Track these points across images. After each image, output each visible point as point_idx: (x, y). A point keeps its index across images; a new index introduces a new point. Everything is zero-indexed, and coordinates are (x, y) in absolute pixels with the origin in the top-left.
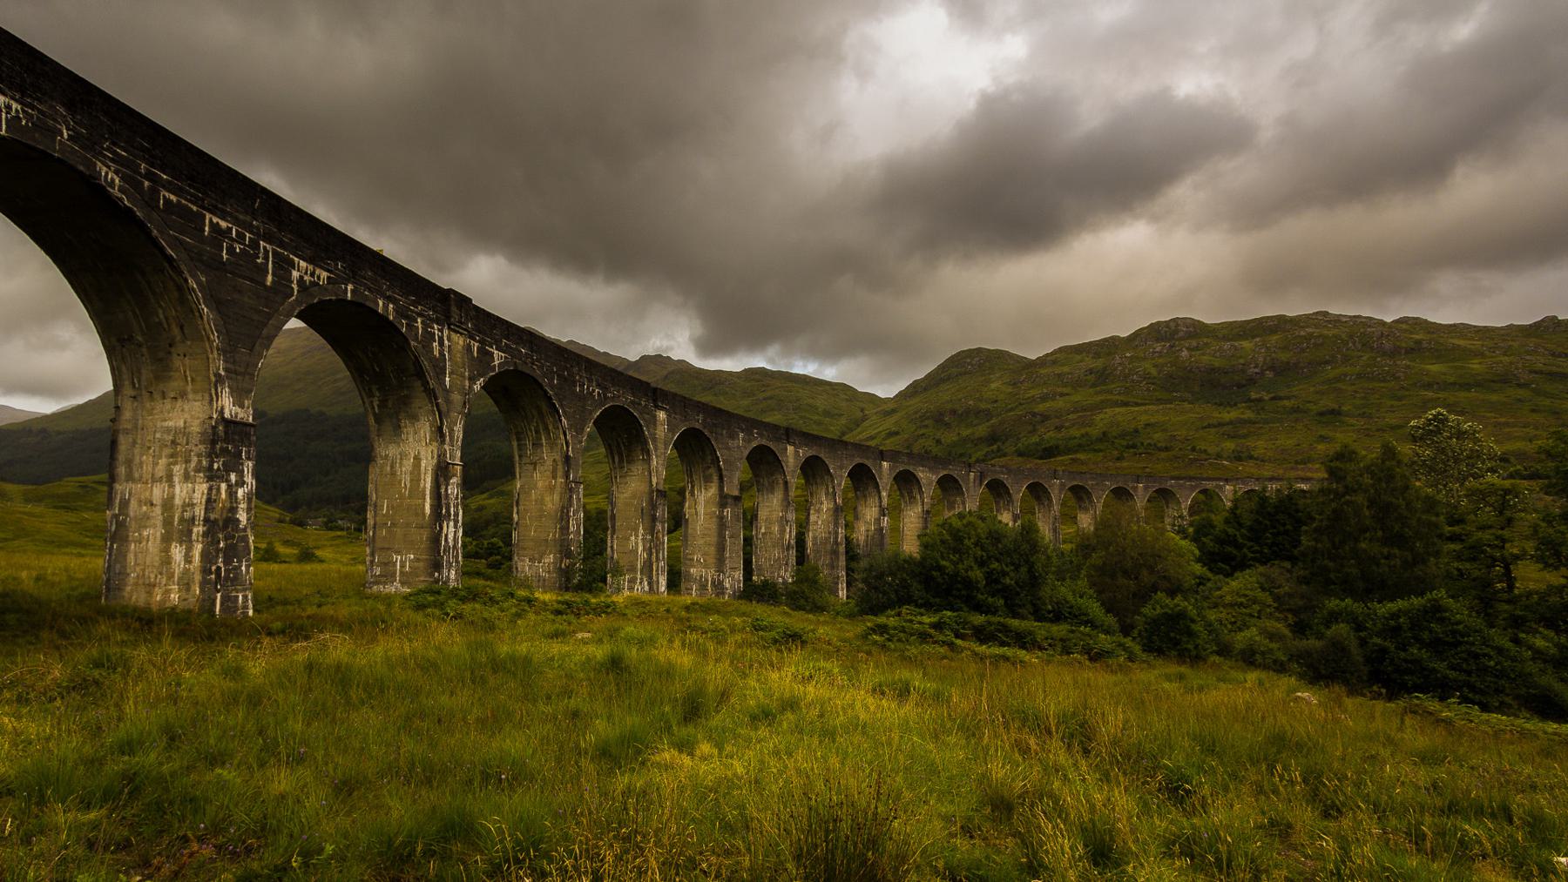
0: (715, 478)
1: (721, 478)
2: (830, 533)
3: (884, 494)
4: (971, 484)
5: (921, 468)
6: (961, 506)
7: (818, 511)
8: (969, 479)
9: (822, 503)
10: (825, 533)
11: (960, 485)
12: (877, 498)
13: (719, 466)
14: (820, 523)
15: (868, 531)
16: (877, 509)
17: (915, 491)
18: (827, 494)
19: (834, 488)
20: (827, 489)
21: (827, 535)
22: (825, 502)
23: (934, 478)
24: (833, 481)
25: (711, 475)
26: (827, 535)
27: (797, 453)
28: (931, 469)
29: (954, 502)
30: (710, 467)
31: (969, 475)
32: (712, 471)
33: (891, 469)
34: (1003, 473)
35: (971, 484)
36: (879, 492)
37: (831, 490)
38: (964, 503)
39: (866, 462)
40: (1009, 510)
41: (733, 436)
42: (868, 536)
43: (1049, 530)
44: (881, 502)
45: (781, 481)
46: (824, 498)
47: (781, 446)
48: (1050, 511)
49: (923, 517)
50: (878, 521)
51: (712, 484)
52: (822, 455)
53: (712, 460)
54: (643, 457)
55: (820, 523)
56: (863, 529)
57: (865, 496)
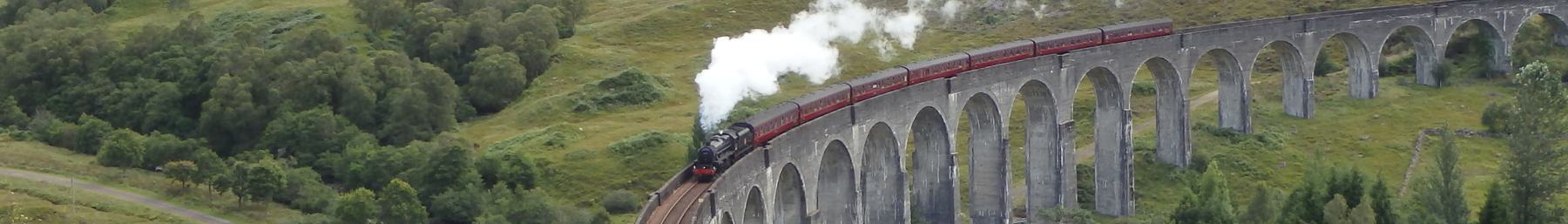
0: (797, 200)
1: (803, 199)
2: (892, 206)
3: (952, 136)
4: (1063, 85)
5: (996, 85)
6: (1049, 117)
7: (877, 179)
8: (1059, 80)
9: (881, 169)
10: (886, 205)
11: (1048, 91)
12: (943, 142)
13: (802, 189)
14: (879, 193)
15: (932, 184)
16: (944, 155)
17: (989, 113)
18: (888, 158)
19: (897, 152)
20: (888, 150)
21: (889, 209)
22: (885, 168)
23: (1014, 92)
24: (895, 143)
25: (792, 196)
26: (889, 209)
27: (861, 129)
28: (1009, 82)
29: (1040, 110)
30: (790, 189)
31: (1059, 73)
32: (794, 193)
33: (959, 99)
34: (1107, 57)
35: (1063, 85)
36: (946, 135)
37: (892, 154)
38: (1053, 113)
39: (930, 103)
41: (810, 153)
42: (931, 191)
43: (1174, 121)
44: (948, 147)
45: (845, 169)
46: (883, 163)
47: (847, 132)
48: (1175, 94)
49: (1000, 149)
50: (946, 172)
51: (793, 206)
52: (884, 120)
53: (794, 183)
54: (756, 215)
55: (879, 193)
56: (925, 181)
57: (927, 139)
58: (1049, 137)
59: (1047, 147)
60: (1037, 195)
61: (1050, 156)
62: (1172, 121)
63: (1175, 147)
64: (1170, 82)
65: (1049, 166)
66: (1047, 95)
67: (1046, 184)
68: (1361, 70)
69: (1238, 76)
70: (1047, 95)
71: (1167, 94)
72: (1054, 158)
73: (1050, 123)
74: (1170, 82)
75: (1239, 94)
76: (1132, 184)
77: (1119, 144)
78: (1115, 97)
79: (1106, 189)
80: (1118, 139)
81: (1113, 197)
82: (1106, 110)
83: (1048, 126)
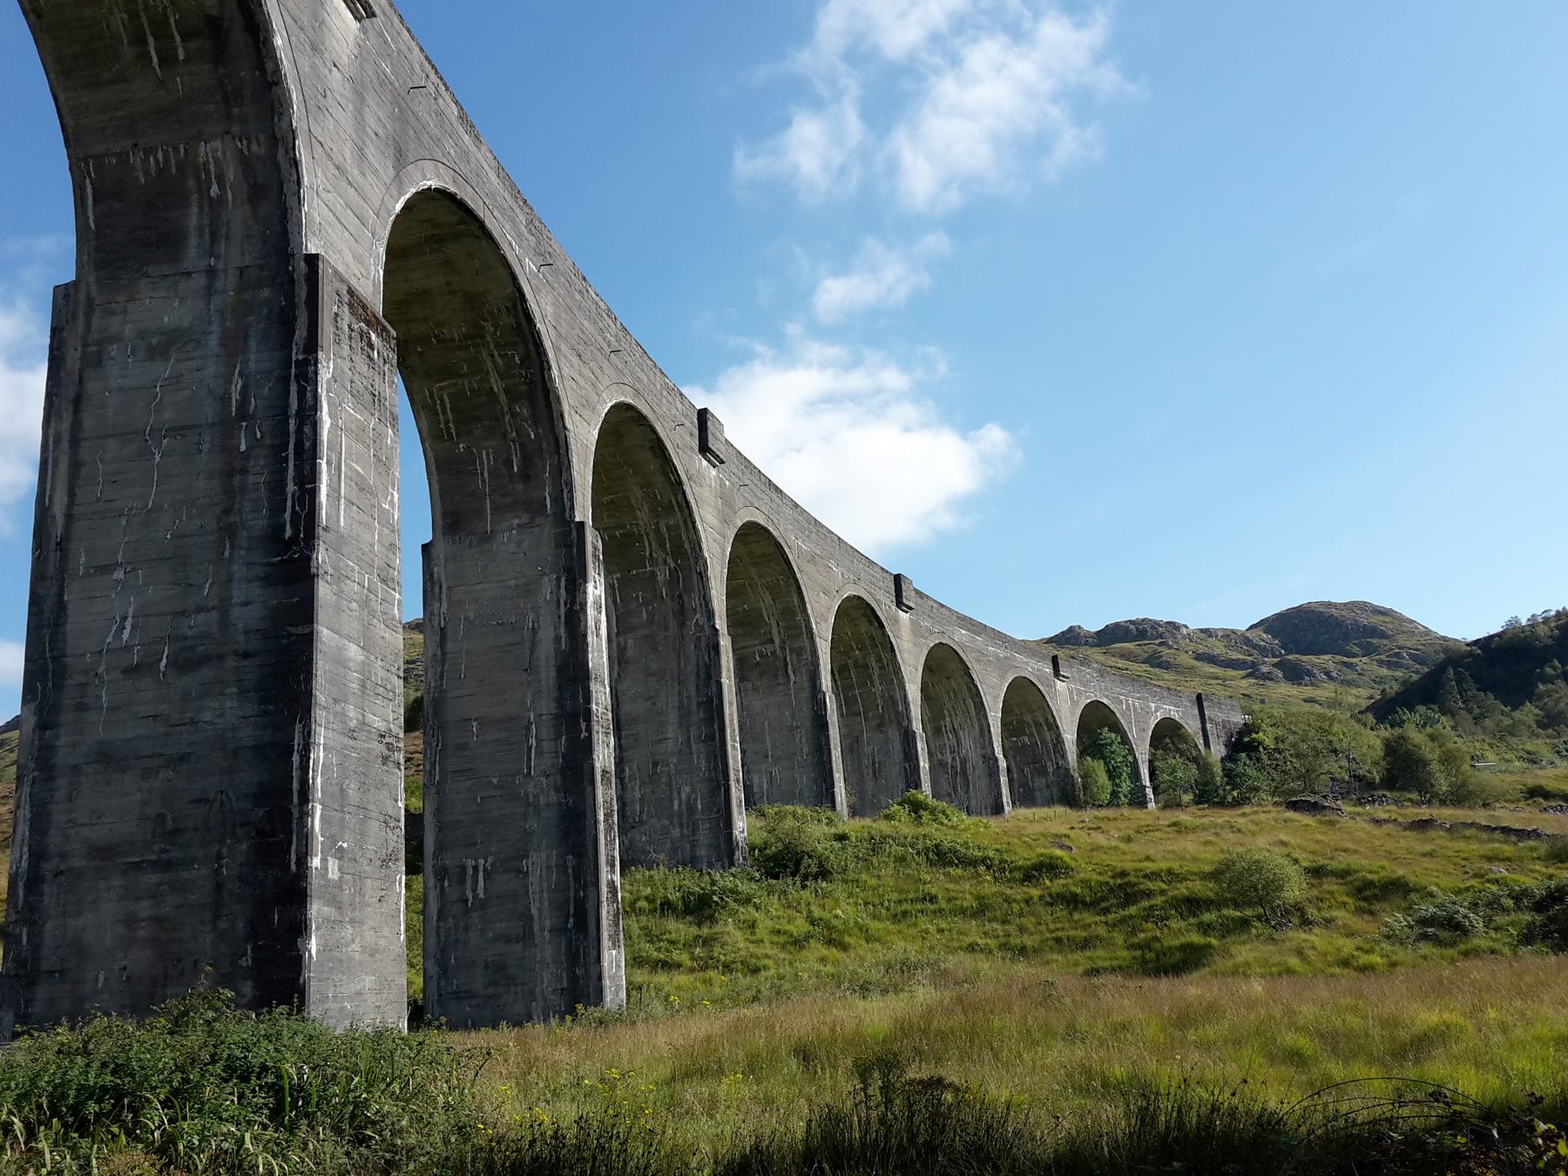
40: (536, 508)
43: (684, 712)
58: (234, 345)
59: (209, 412)
60: (109, 758)
61: (232, 470)
62: (673, 716)
63: (691, 808)
64: (662, 575)
65: (228, 531)
66: (239, 37)
67: (184, 663)
68: (964, 762)
69: (799, 652)
70: (239, 37)
71: (651, 621)
72: (258, 477)
73: (237, 254)
74: (662, 575)
75: (806, 708)
76: (613, 871)
77: (548, 676)
78: (525, 477)
79: (482, 905)
80: (546, 651)
81: (526, 936)
82: (487, 538)
83: (227, 283)
